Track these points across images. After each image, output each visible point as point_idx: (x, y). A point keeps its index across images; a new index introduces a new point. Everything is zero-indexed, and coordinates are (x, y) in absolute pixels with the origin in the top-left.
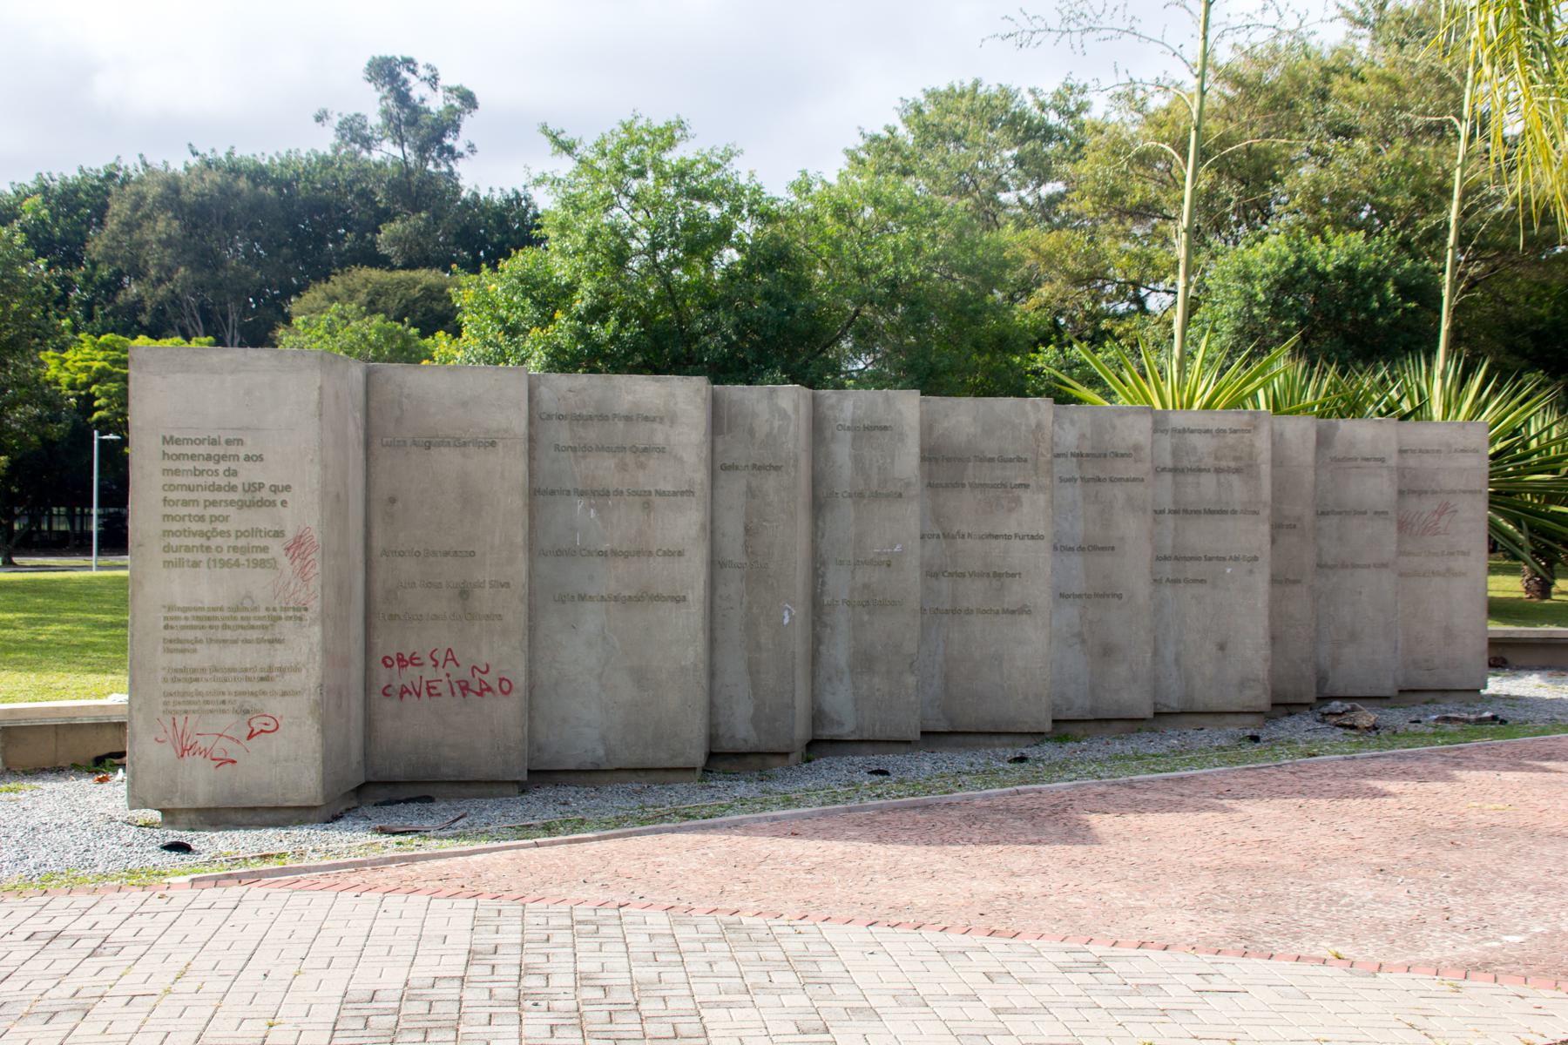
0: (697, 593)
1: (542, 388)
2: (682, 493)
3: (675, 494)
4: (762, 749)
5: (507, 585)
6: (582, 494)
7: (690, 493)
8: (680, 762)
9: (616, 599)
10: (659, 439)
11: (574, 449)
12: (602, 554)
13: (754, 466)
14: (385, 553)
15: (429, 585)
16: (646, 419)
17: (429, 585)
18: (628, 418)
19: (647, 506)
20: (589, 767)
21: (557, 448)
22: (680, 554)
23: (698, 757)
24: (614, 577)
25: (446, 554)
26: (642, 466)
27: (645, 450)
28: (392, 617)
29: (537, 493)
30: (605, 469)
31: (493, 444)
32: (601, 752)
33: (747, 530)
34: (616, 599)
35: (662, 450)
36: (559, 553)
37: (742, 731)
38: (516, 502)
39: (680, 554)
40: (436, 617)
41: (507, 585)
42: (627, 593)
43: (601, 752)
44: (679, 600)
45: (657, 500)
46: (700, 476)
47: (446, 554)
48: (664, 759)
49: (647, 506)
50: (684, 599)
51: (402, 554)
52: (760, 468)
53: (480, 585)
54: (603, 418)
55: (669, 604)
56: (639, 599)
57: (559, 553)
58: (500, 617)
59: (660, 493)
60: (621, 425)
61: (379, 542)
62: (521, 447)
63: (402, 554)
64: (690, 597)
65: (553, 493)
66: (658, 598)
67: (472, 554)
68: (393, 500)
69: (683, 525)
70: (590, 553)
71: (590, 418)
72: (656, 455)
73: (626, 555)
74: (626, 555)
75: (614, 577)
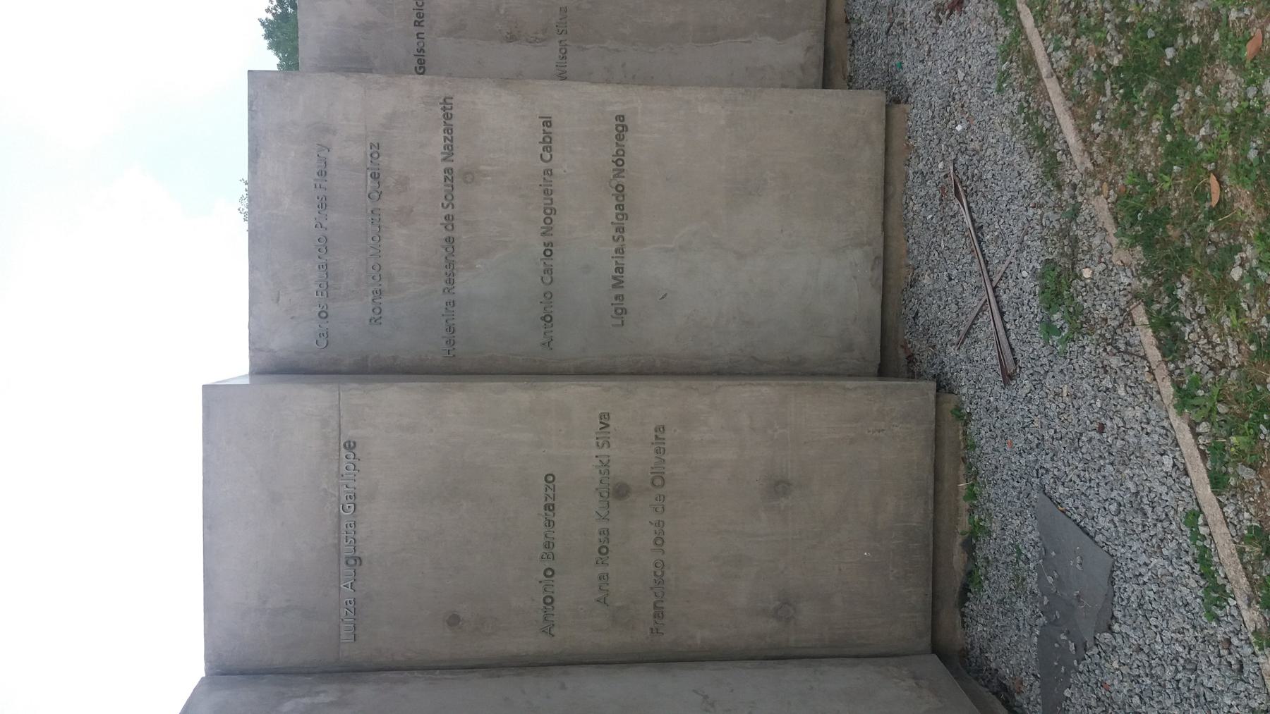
0: (614, 98)
1: (274, 345)
2: (448, 117)
3: (449, 129)
4: (820, 24)
5: (604, 420)
6: (450, 281)
7: (447, 104)
8: (877, 129)
9: (620, 229)
10: (357, 153)
11: (379, 293)
12: (548, 252)
13: (418, 24)
14: (548, 631)
15: (603, 551)
16: (322, 173)
17: (603, 551)
18: (323, 205)
19: (471, 176)
20: (879, 271)
21: (374, 321)
22: (548, 123)
23: (869, 102)
24: (586, 233)
25: (550, 524)
26: (403, 183)
27: (375, 176)
28: (659, 614)
29: (450, 366)
30: (409, 245)
31: (350, 446)
32: (856, 255)
33: (511, 38)
34: (620, 229)
35: (376, 147)
36: (547, 319)
37: (798, 50)
38: (459, 402)
39: (548, 123)
40: (659, 540)
41: (604, 420)
42: (612, 213)
43: (856, 255)
44: (622, 126)
45: (461, 158)
46: (418, 85)
47: (550, 524)
48: (870, 156)
49: (471, 176)
50: (620, 118)
51: (549, 601)
52: (420, 16)
53: (605, 465)
54: (324, 245)
55: (629, 143)
56: (620, 191)
57: (547, 319)
58: (660, 429)
59: (449, 151)
60: (334, 217)
61: (528, 642)
62: (356, 395)
63: (549, 601)
64: (618, 109)
65: (451, 329)
66: (619, 161)
67: (550, 479)
68: (454, 620)
69: (500, 117)
70: (549, 271)
71: (324, 267)
72: (383, 160)
73: (550, 212)
74: (550, 212)
75: (586, 233)
